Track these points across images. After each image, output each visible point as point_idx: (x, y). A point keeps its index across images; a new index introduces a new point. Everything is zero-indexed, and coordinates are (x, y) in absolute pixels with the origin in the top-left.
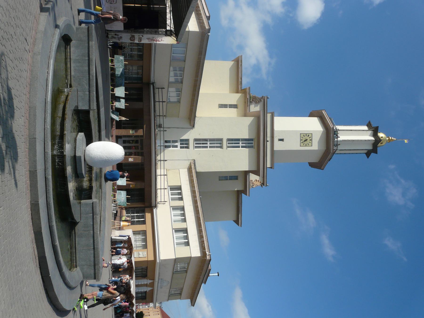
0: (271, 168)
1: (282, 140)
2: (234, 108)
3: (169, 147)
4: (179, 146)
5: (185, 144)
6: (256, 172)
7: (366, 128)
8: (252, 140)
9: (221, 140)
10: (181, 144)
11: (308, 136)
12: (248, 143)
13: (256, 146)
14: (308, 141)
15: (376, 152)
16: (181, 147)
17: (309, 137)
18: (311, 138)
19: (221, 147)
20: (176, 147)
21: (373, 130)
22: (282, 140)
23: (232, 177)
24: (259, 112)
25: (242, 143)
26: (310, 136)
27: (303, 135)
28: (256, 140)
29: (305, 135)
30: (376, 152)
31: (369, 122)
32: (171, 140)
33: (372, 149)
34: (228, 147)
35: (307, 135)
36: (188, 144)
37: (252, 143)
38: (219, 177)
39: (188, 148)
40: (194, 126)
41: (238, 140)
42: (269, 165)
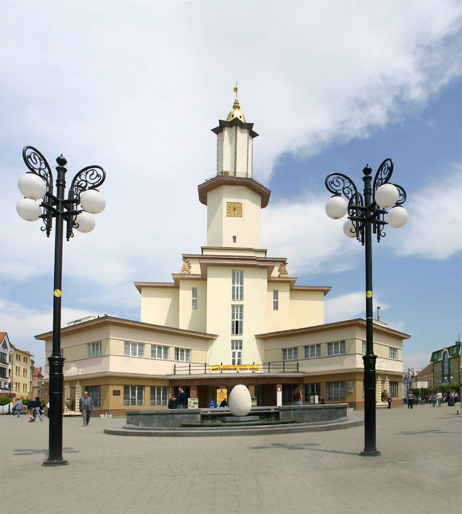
0: (265, 252)
1: (234, 238)
2: (196, 292)
3: (239, 361)
4: (239, 350)
5: (237, 345)
6: (270, 269)
9: (233, 306)
10: (237, 348)
12: (238, 279)
15: (252, 125)
16: (241, 348)
19: (241, 306)
20: (239, 354)
21: (224, 127)
22: (234, 238)
23: (274, 296)
24: (201, 264)
25: (238, 284)
26: (230, 205)
28: (235, 268)
29: (229, 211)
30: (252, 125)
31: (212, 130)
32: (232, 358)
33: (248, 129)
34: (242, 298)
36: (237, 341)
37: (238, 273)
38: (274, 309)
39: (241, 342)
40: (217, 336)
41: (233, 288)
42: (263, 256)
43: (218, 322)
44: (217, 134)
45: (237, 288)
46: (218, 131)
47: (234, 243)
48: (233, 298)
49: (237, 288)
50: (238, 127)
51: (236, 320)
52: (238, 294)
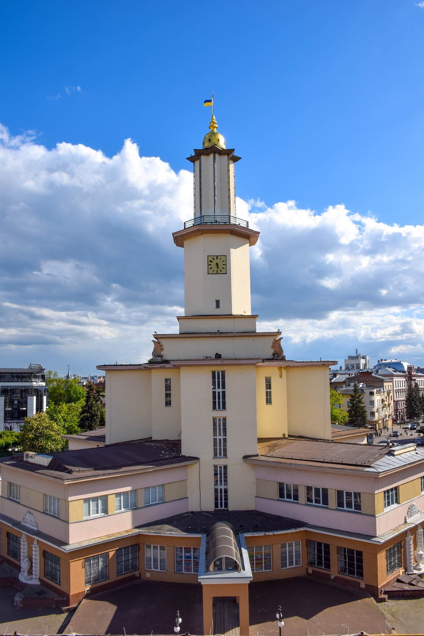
1: (218, 302)
7: (197, 163)
8: (214, 373)
11: (211, 261)
13: (223, 368)
14: (218, 261)
17: (212, 260)
18: (215, 258)
21: (200, 155)
22: (218, 302)
26: (210, 259)
27: (210, 270)
29: (210, 267)
34: (224, 408)
35: (210, 263)
37: (218, 373)
43: (196, 440)
44: (194, 162)
45: (219, 393)
46: (192, 159)
47: (218, 309)
48: (214, 408)
49: (219, 393)
50: (216, 155)
51: (218, 437)
52: (219, 401)
